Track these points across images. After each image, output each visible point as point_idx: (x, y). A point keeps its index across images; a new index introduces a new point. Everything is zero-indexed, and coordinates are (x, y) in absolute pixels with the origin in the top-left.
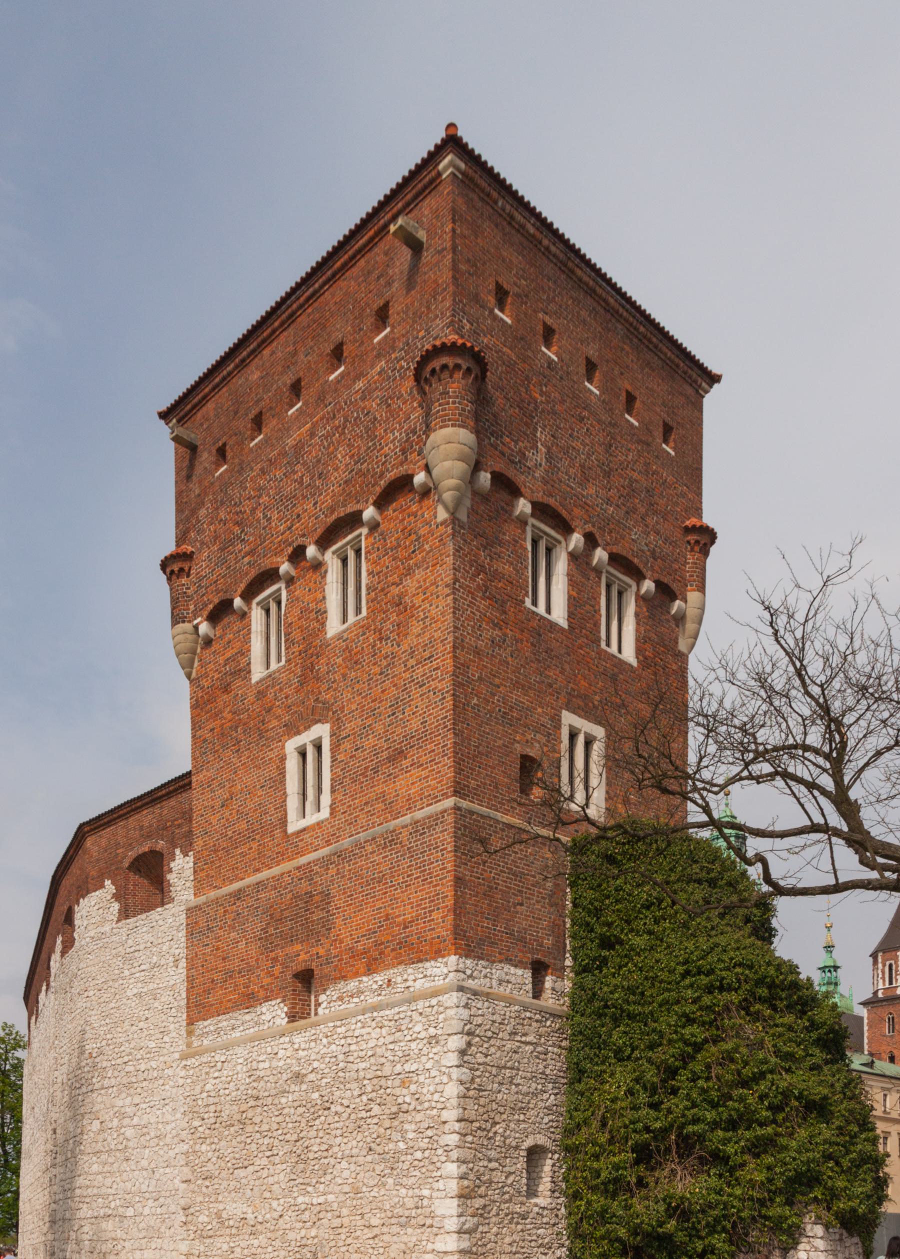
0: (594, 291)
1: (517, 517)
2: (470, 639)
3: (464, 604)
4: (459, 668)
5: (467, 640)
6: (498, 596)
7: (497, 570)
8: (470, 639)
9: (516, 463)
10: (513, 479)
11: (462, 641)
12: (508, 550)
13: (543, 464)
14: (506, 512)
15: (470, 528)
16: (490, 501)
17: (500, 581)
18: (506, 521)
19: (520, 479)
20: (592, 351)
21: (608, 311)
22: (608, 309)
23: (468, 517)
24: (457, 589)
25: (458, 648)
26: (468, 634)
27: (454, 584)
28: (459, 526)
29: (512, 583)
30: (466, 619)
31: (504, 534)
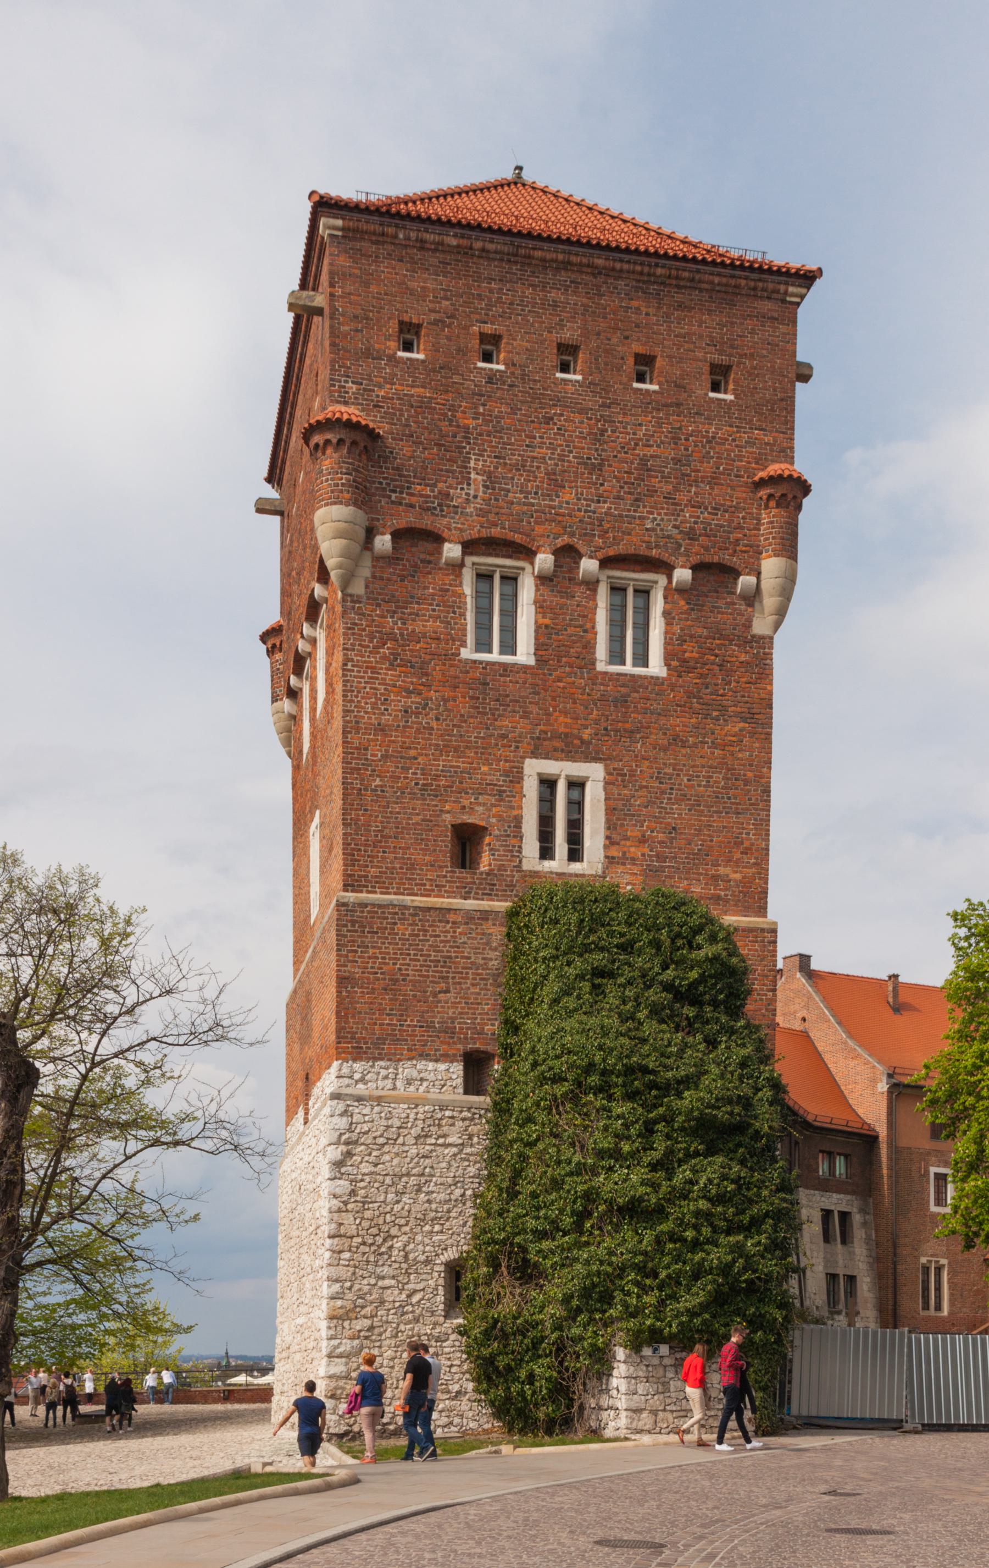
0: (569, 263)
1: (447, 564)
2: (370, 718)
3: (360, 682)
4: (353, 753)
5: (366, 720)
6: (413, 660)
7: (414, 631)
8: (370, 718)
9: (435, 508)
10: (429, 528)
11: (357, 722)
12: (431, 604)
13: (481, 494)
14: (430, 562)
15: (368, 598)
16: (403, 560)
17: (419, 642)
18: (429, 573)
19: (439, 524)
20: (569, 334)
21: (600, 273)
22: (596, 272)
23: (367, 587)
24: (349, 670)
25: (351, 732)
26: (366, 713)
27: (345, 665)
28: (353, 601)
29: (438, 639)
30: (363, 698)
31: (426, 588)
